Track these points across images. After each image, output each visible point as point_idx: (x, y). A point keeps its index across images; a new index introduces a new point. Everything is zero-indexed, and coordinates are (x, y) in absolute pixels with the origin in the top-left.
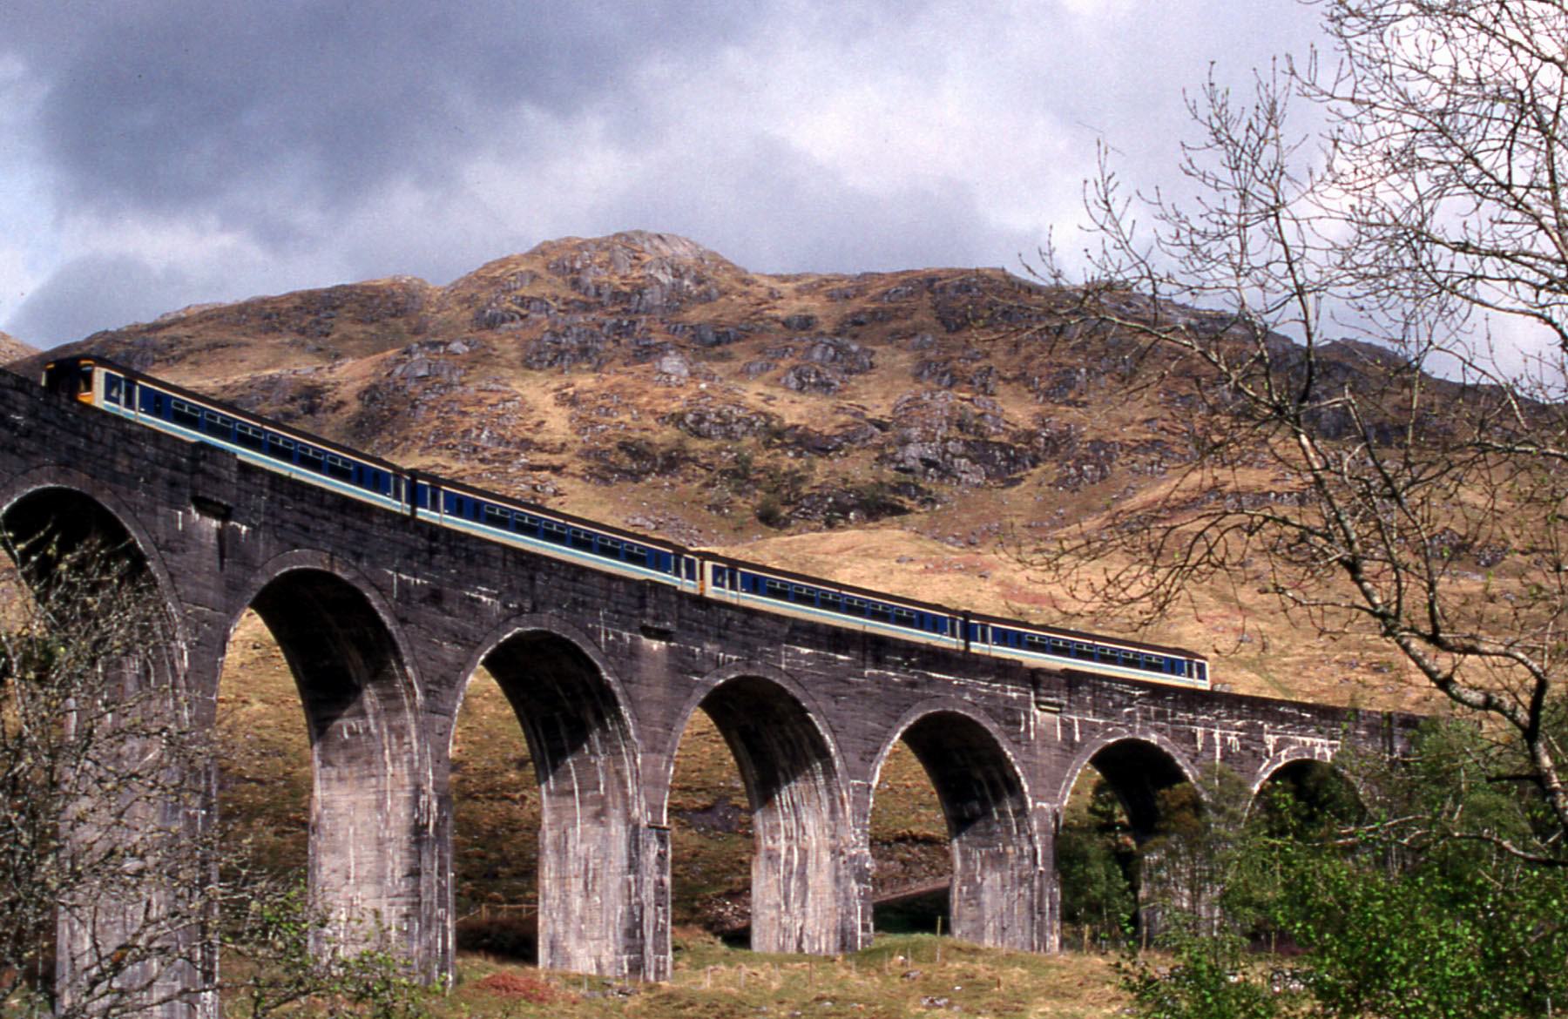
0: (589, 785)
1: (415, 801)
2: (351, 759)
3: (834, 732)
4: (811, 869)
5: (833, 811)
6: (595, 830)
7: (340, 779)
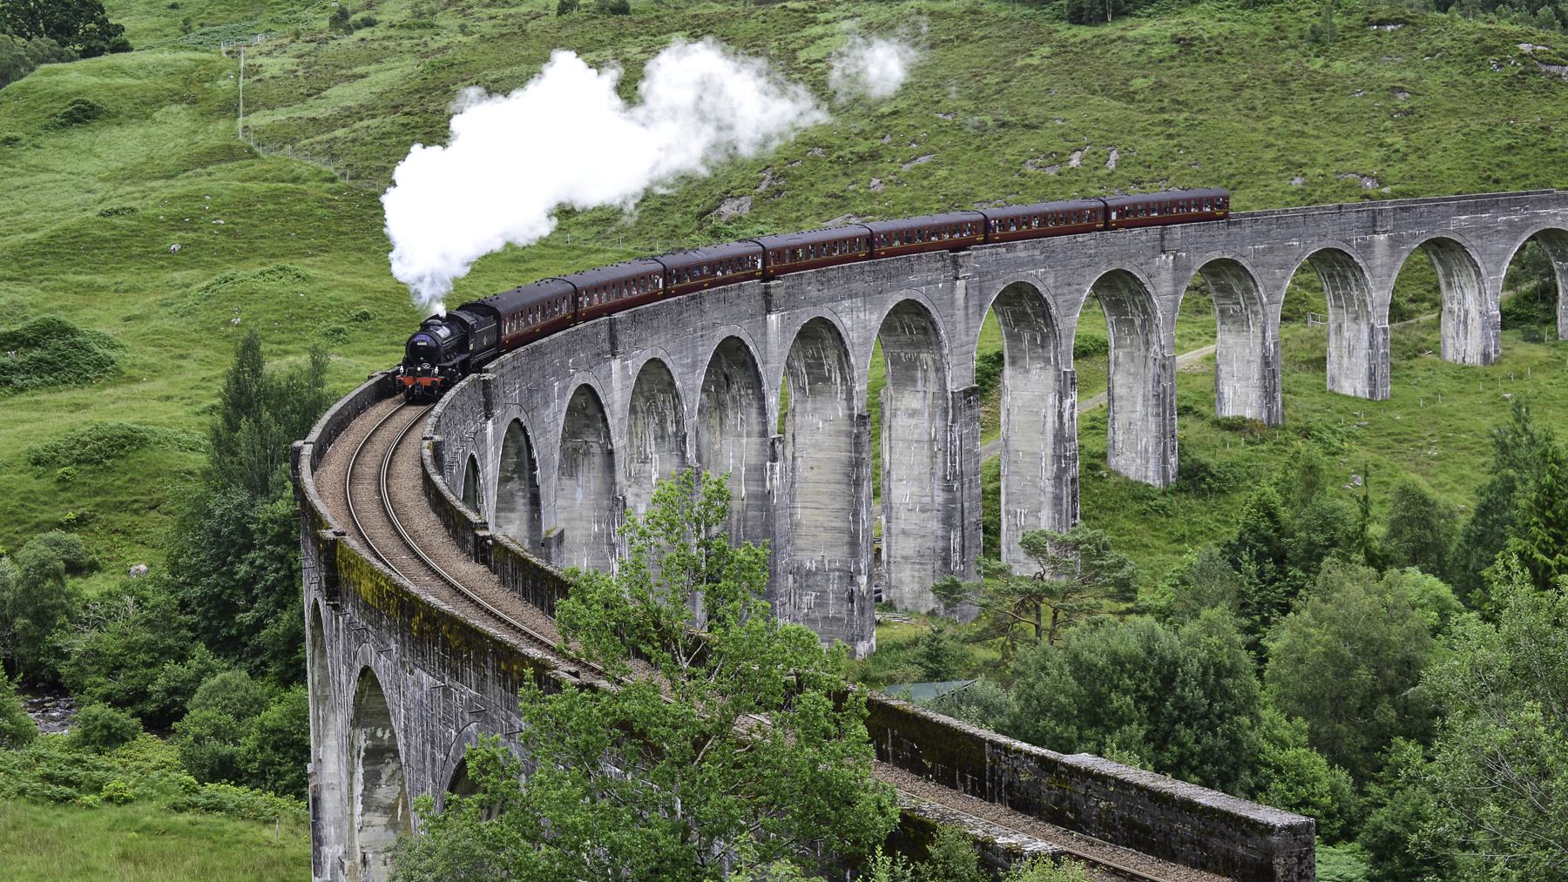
1: (1263, 344)
2: (1234, 323)
3: (1480, 255)
4: (1469, 321)
5: (1480, 293)
6: (1354, 326)
7: (1230, 331)
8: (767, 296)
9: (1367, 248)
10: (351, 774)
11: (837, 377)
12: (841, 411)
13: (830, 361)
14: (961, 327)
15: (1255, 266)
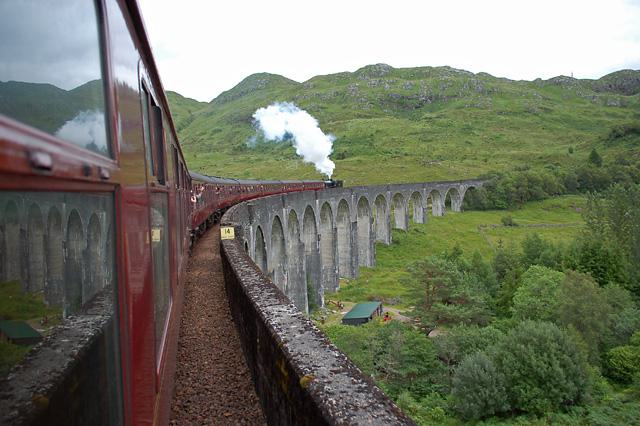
8: (316, 194)
9: (422, 191)
11: (329, 218)
12: (330, 227)
13: (327, 214)
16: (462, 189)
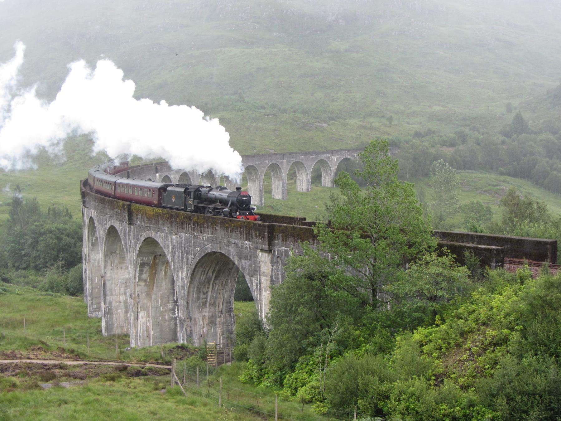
0: (277, 177)
9: (282, 163)
10: (136, 270)
14: (195, 180)
15: (258, 167)
16: (334, 161)
